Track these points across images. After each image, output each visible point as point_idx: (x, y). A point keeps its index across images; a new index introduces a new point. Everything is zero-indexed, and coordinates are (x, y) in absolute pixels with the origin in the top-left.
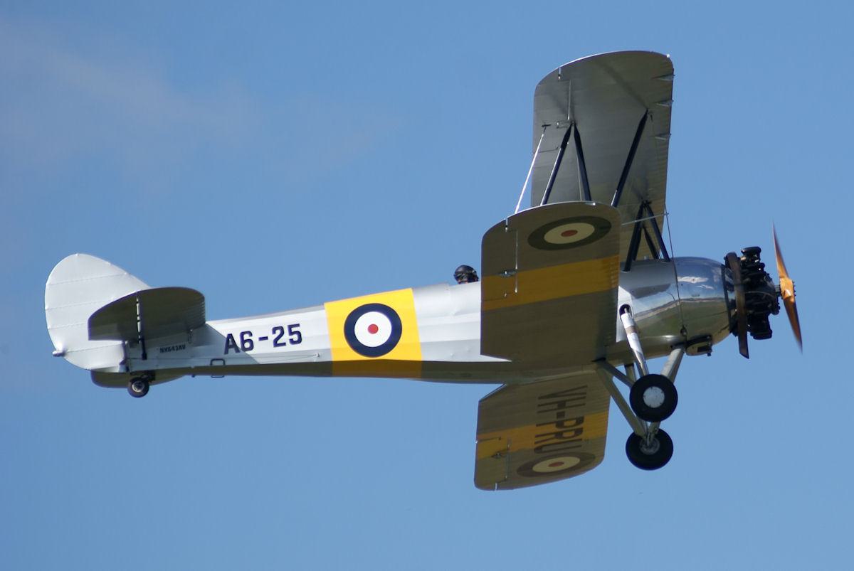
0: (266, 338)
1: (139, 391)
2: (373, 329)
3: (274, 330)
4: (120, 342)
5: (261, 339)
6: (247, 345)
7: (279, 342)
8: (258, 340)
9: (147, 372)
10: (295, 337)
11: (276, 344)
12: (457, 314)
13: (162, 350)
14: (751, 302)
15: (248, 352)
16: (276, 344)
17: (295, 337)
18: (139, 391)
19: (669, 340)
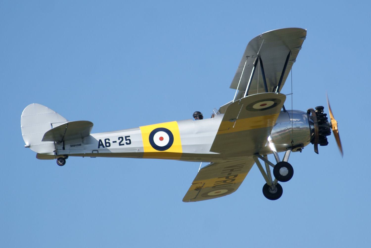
0: (116, 142)
1: (61, 163)
2: (161, 139)
3: (119, 138)
4: (53, 142)
5: (114, 142)
6: (108, 145)
7: (121, 143)
8: (112, 142)
9: (64, 155)
10: (128, 142)
11: (120, 144)
12: (197, 133)
13: (71, 146)
14: (320, 130)
15: (108, 148)
16: (120, 144)
17: (128, 142)
18: (61, 163)
19: (285, 146)
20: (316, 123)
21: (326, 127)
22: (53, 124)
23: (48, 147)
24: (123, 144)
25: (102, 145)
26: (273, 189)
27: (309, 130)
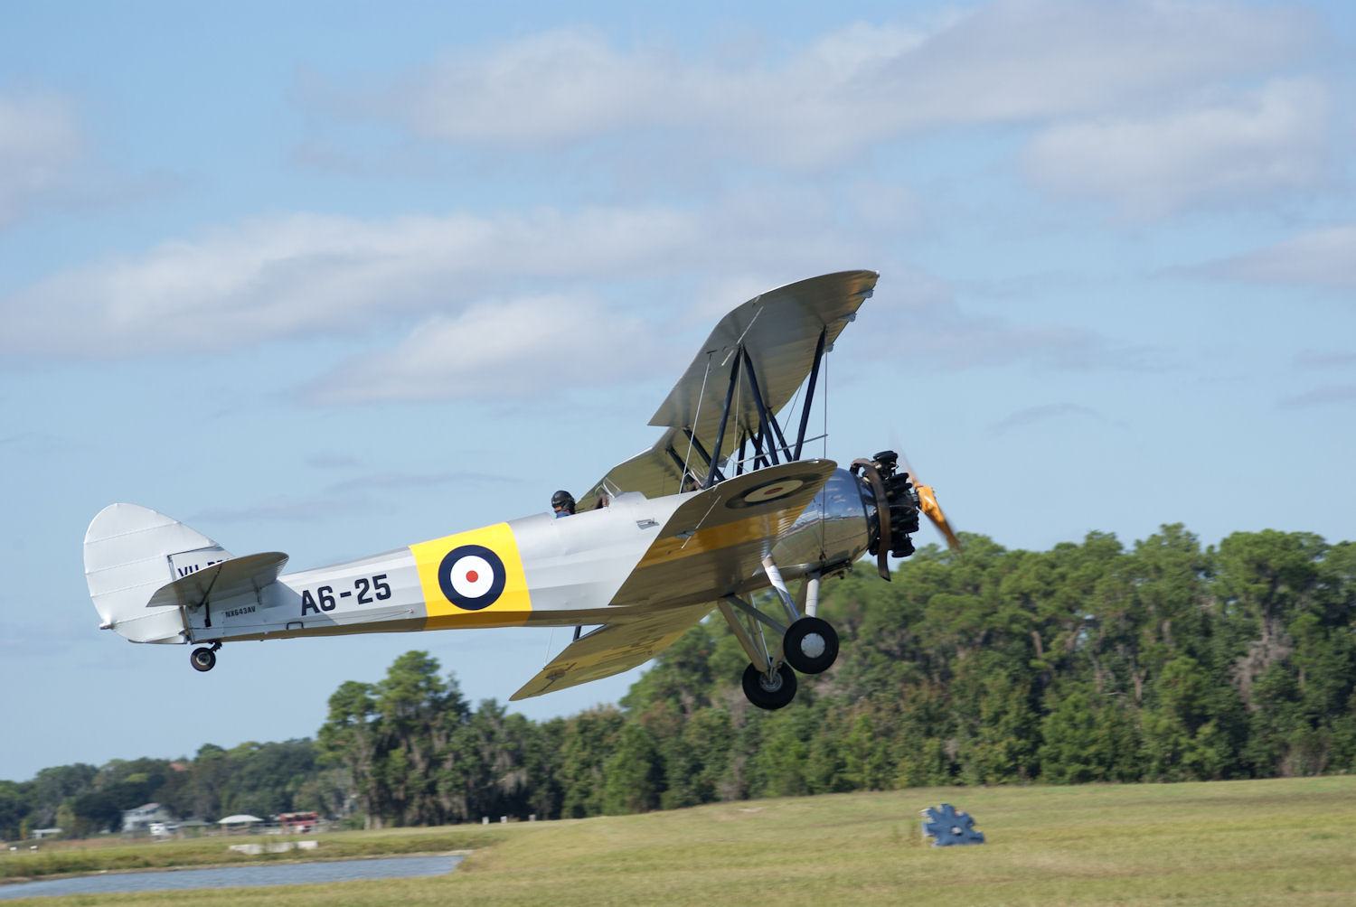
0: (348, 594)
1: (203, 664)
2: (472, 577)
3: (357, 583)
4: (177, 607)
5: (343, 595)
6: (327, 603)
7: (365, 597)
11: (361, 601)
12: (568, 553)
16: (361, 601)
17: (383, 591)
18: (203, 664)
20: (882, 501)
21: (910, 509)
22: (173, 558)
23: (167, 621)
24: (370, 600)
25: (313, 604)
26: (771, 681)
27: (864, 521)
